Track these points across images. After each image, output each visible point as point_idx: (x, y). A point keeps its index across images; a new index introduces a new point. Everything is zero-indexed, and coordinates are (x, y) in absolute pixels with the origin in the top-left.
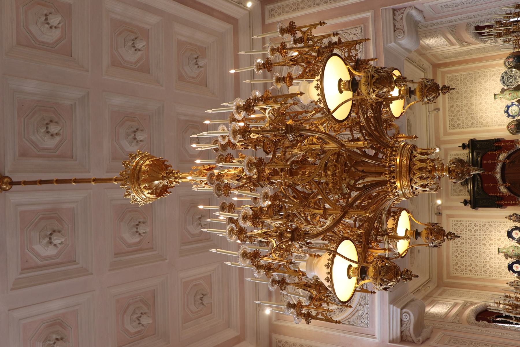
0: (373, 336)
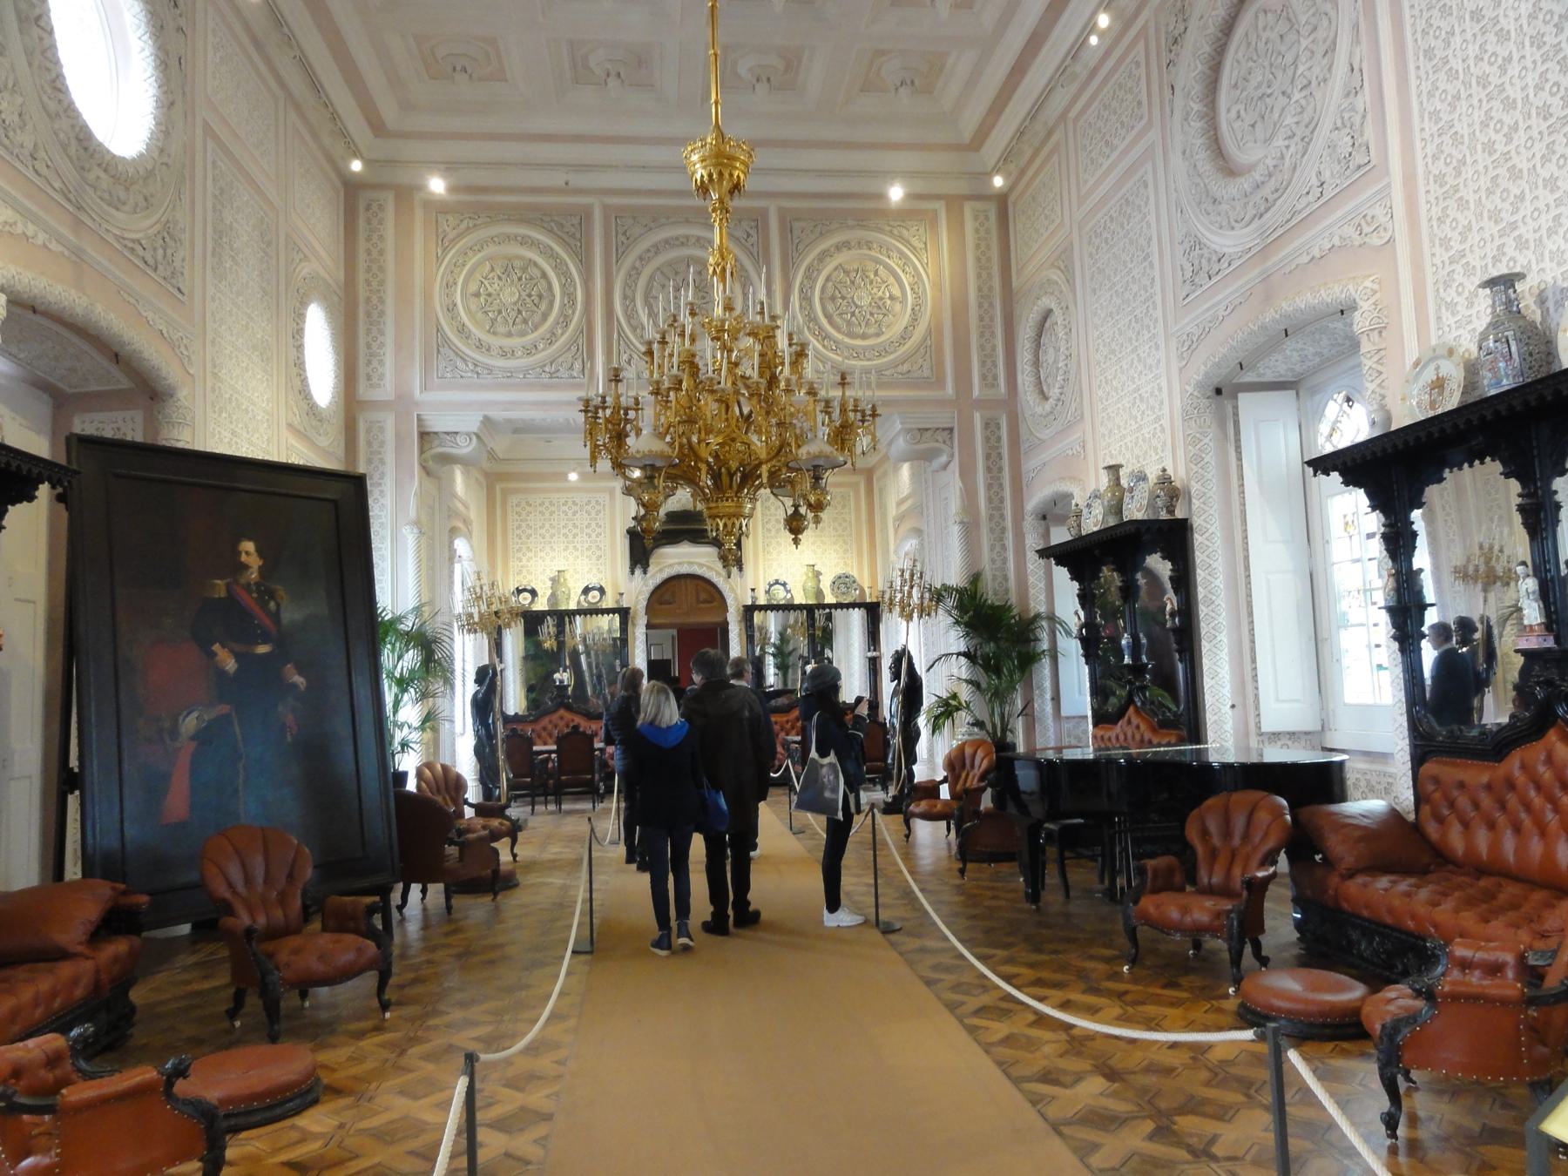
0: (425, 388)
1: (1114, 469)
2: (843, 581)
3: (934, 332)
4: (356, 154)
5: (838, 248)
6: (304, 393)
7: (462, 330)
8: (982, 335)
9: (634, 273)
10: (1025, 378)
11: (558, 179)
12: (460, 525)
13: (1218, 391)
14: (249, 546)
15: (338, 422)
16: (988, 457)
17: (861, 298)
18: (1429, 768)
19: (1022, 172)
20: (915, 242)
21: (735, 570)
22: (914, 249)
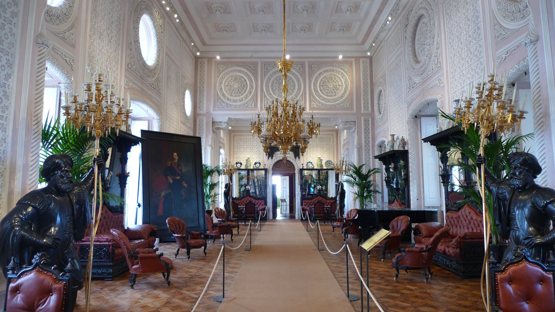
0: (214, 110)
1: (393, 136)
2: (328, 162)
3: (351, 94)
4: (198, 51)
5: (324, 72)
6: (185, 113)
7: (224, 95)
8: (364, 95)
9: (269, 79)
10: (376, 108)
11: (249, 55)
12: (222, 145)
13: (416, 117)
14: (175, 154)
15: (192, 120)
16: (365, 129)
18: (448, 213)
19: (375, 51)
21: (297, 158)
22: (346, 72)
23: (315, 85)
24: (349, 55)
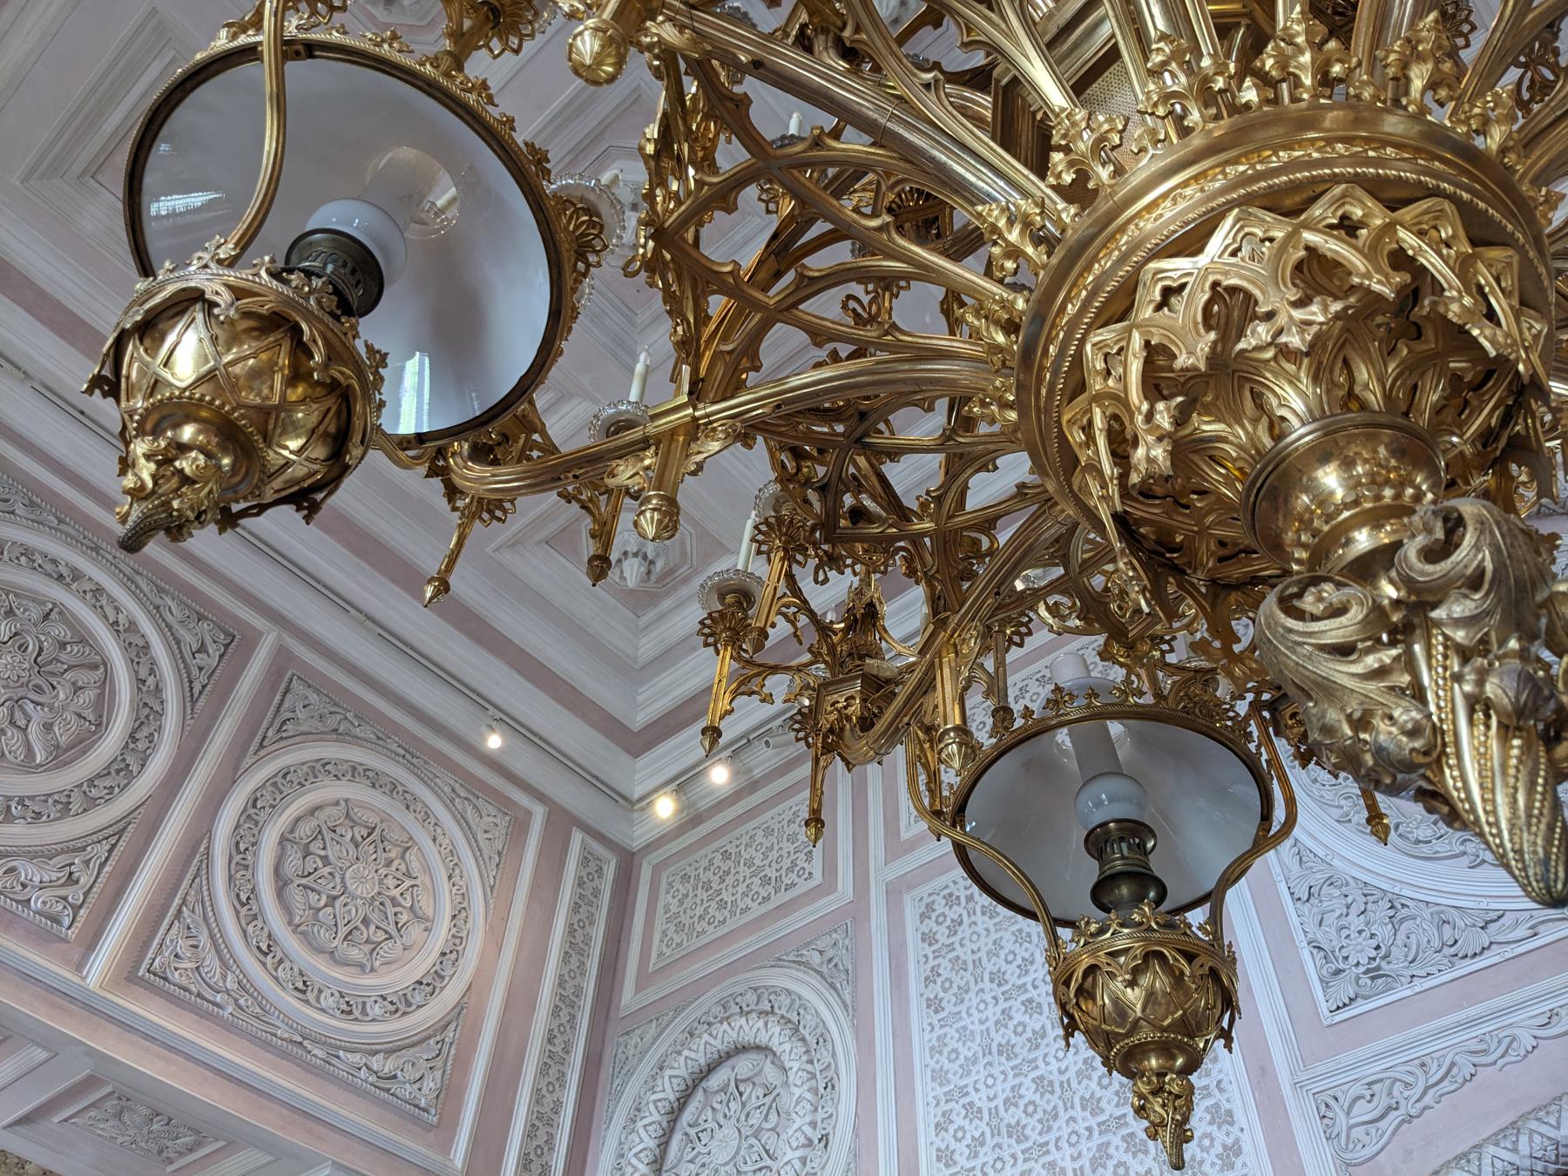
5: (355, 771)
17: (362, 880)
20: (481, 837)
23: (252, 815)
24: (527, 764)
